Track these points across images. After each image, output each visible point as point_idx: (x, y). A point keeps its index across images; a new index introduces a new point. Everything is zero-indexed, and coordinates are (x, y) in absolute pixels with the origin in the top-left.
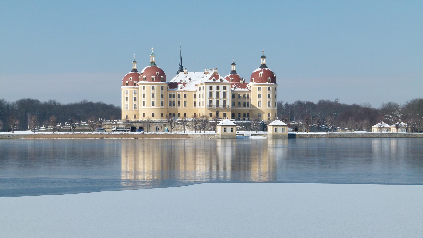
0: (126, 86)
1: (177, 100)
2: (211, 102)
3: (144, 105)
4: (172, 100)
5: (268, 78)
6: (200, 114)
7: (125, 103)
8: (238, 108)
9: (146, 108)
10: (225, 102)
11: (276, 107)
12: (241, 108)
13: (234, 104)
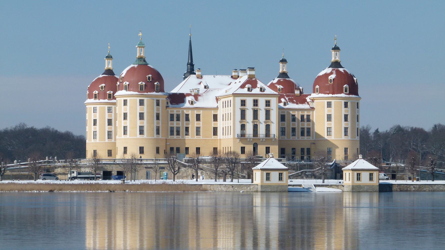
1: (183, 124)
2: (243, 127)
3: (125, 133)
4: (175, 124)
5: (344, 86)
6: (224, 148)
7: (93, 130)
8: (292, 138)
9: (128, 139)
10: (268, 127)
11: (359, 137)
12: (296, 138)
13: (285, 132)
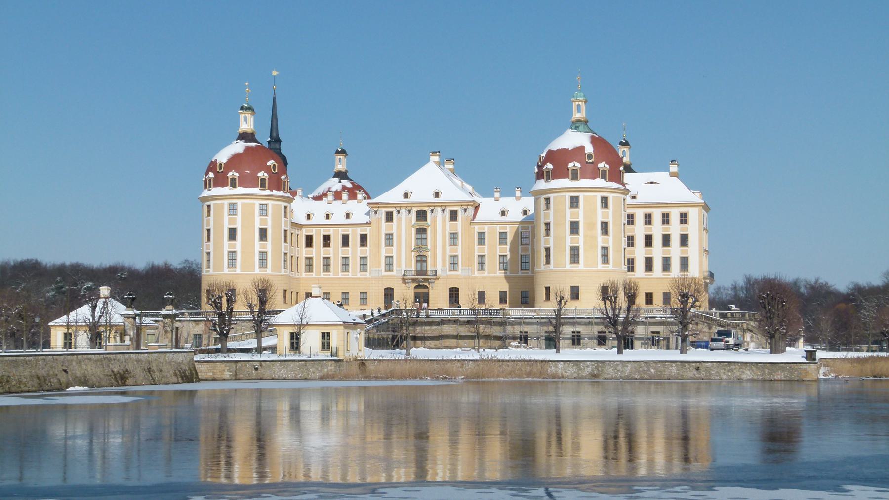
0: (259, 188)
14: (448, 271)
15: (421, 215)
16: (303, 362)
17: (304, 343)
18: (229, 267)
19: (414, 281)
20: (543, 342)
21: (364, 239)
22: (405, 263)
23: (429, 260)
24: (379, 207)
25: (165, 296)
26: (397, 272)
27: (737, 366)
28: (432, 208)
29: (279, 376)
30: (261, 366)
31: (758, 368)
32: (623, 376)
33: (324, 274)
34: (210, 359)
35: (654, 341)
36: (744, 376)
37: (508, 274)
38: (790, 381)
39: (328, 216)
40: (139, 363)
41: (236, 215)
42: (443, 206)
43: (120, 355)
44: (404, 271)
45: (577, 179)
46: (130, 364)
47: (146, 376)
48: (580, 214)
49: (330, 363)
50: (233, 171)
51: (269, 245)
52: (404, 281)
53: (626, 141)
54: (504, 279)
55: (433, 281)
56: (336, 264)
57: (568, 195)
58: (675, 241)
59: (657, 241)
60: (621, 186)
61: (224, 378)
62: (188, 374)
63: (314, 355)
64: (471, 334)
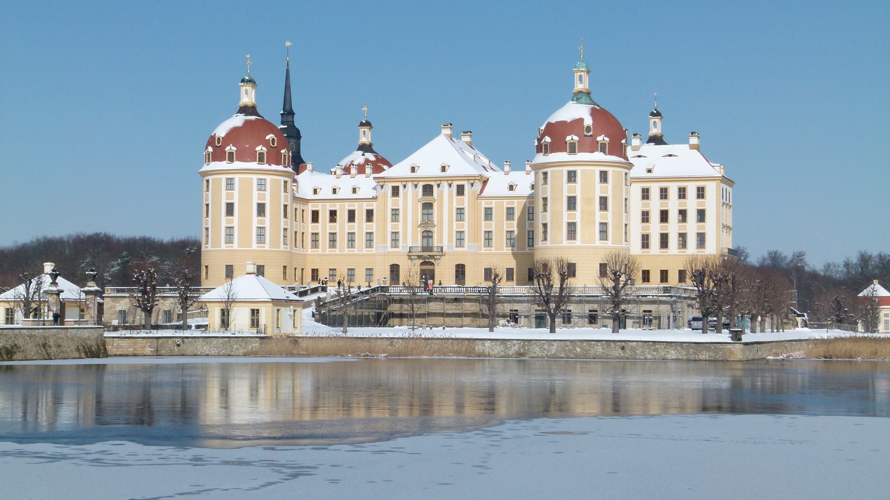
0: (257, 162)
14: (454, 247)
15: (428, 190)
16: (226, 339)
17: (234, 320)
18: (226, 243)
19: (419, 257)
20: (533, 320)
21: (370, 214)
22: (412, 238)
23: (435, 236)
24: (385, 182)
25: (87, 273)
26: (403, 248)
27: (662, 346)
28: (439, 183)
29: (201, 353)
30: (183, 342)
31: (682, 347)
32: (549, 354)
33: (348, 249)
34: (131, 335)
35: (647, 320)
36: (669, 356)
37: (516, 251)
38: (715, 361)
39: (334, 191)
40: (32, 338)
41: (233, 190)
42: (450, 180)
43: (8, 330)
44: (410, 247)
45: (575, 153)
46: (20, 339)
47: (40, 352)
48: (578, 190)
49: (254, 340)
50: (231, 145)
51: (267, 220)
52: (410, 257)
53: (657, 112)
54: (512, 256)
55: (439, 257)
56: (342, 240)
57: (565, 169)
58: (692, 216)
59: (673, 216)
60: (622, 160)
61: (145, 354)
62: (94, 350)
63: (239, 332)
64: (458, 312)
